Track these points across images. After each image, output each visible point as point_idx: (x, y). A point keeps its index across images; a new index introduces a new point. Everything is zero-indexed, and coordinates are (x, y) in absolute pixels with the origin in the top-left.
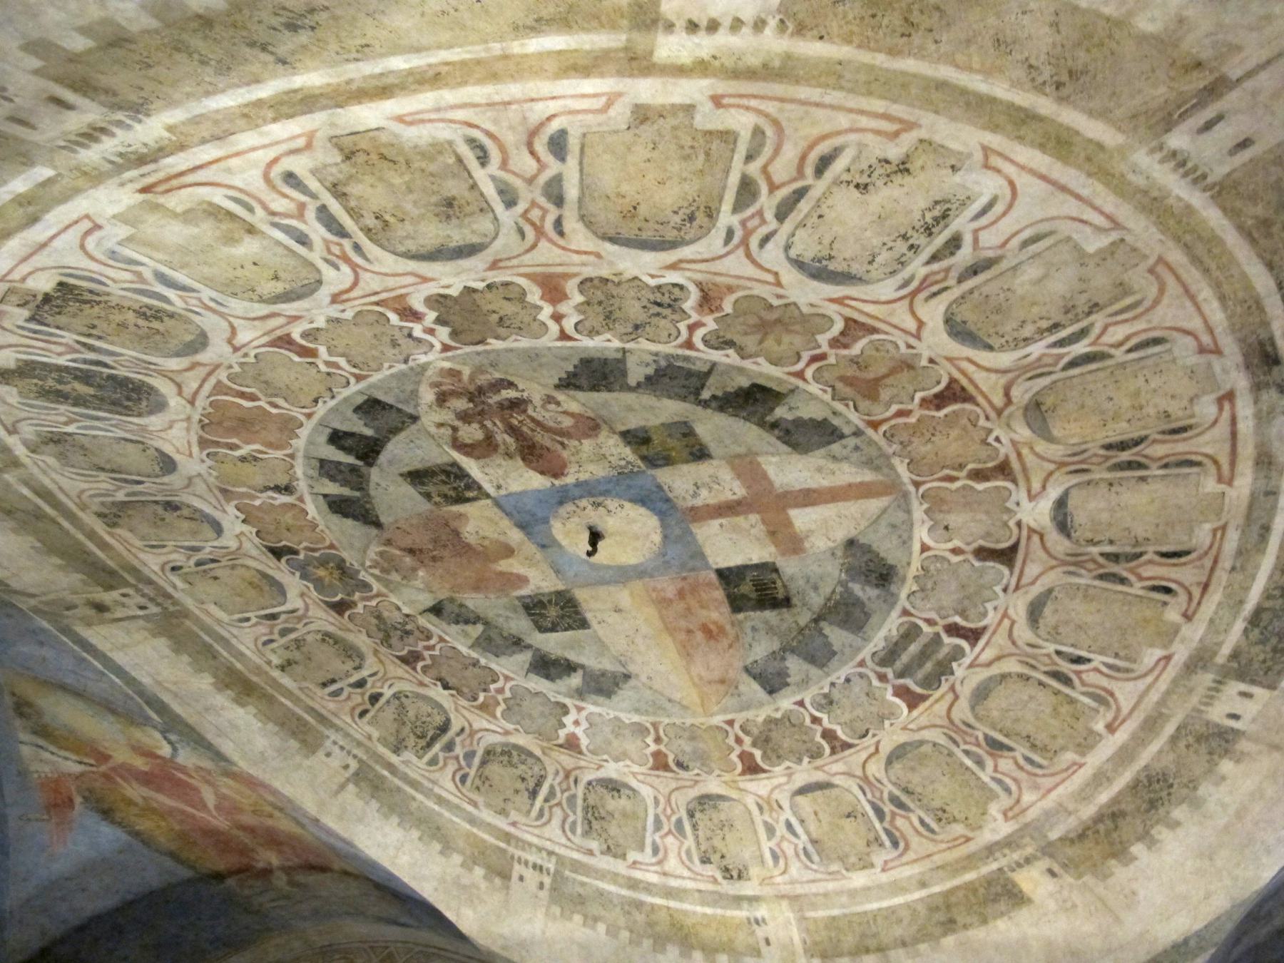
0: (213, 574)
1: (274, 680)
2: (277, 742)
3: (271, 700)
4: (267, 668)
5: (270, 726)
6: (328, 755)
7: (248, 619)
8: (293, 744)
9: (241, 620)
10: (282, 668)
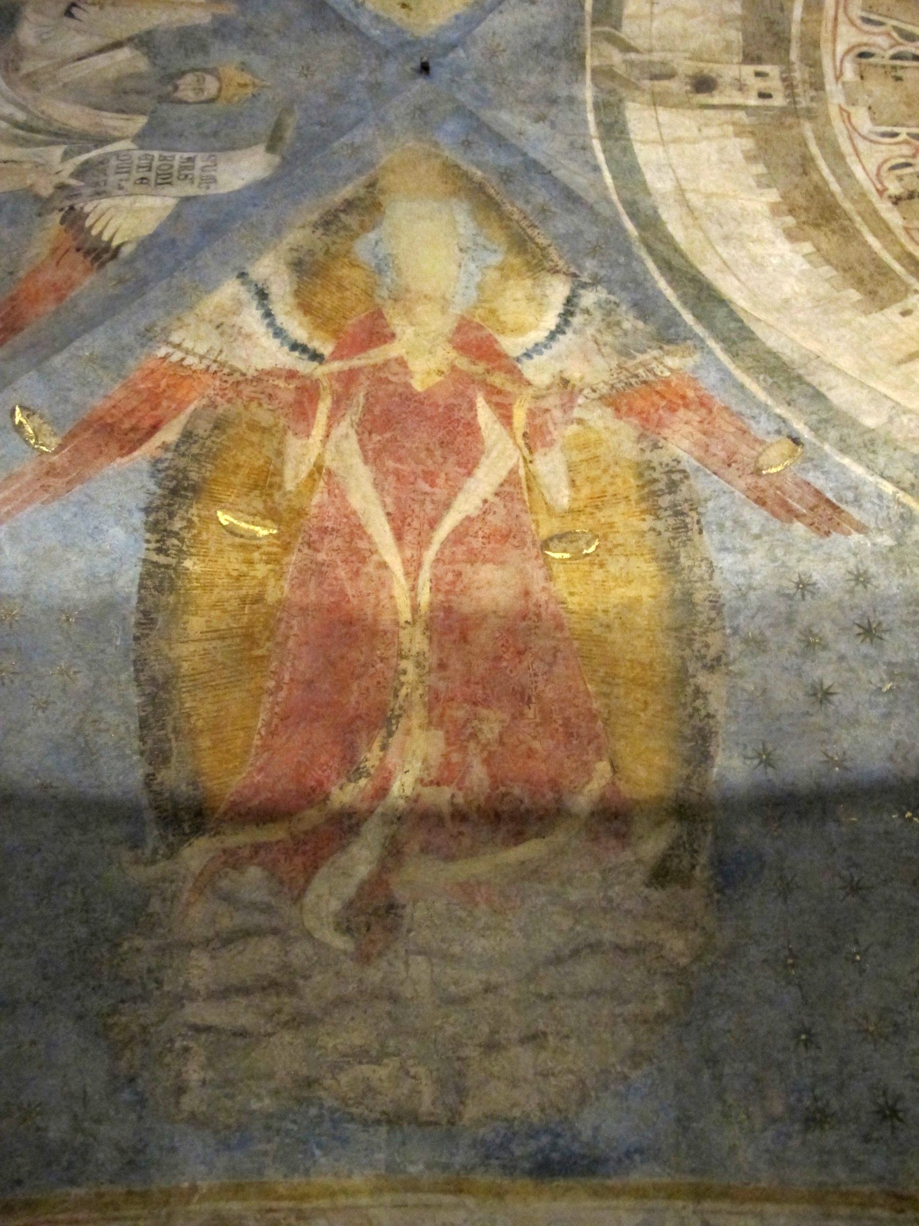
0: (900, 73)
1: (875, 212)
2: (823, 289)
3: (848, 234)
4: (874, 197)
5: (826, 270)
6: (905, 313)
7: (895, 135)
8: (854, 295)
9: (884, 135)
10: (897, 201)
